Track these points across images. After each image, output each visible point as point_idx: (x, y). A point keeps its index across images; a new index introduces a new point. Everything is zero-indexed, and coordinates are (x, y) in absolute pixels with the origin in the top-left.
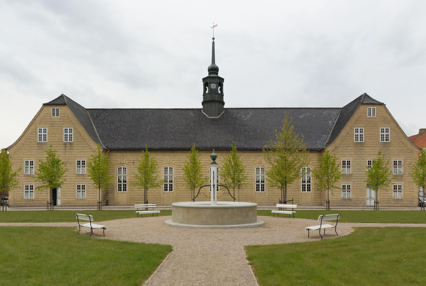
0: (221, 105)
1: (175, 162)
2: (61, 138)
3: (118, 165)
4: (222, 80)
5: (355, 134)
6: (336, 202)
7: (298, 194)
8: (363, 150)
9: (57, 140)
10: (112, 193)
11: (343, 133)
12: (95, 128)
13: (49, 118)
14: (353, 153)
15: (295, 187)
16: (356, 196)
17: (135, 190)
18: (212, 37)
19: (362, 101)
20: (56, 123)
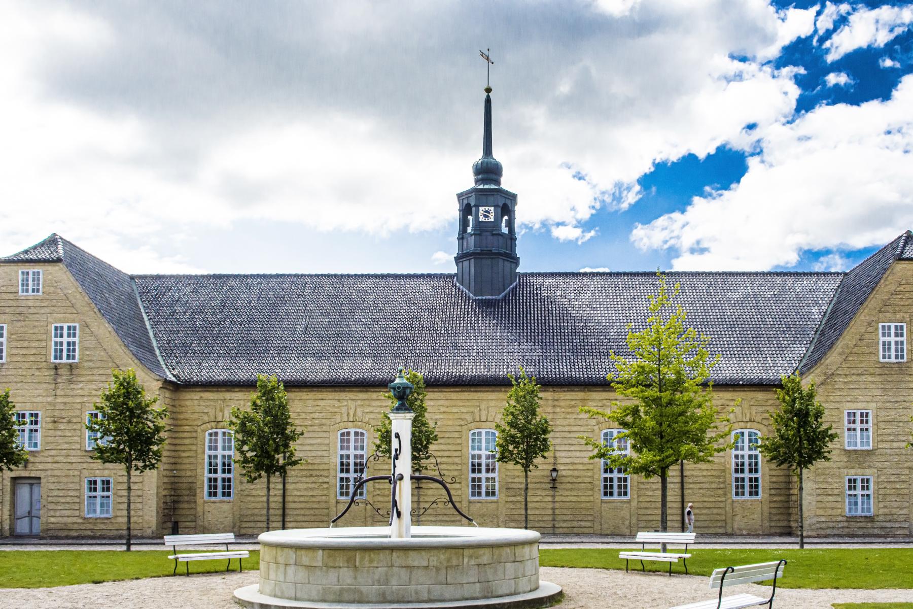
0: (507, 264)
1: (372, 416)
2: (44, 352)
3: (209, 425)
4: (513, 197)
5: (882, 339)
6: (831, 525)
7: (722, 505)
8: (903, 385)
9: (32, 358)
10: (188, 502)
11: (847, 339)
12: (148, 327)
13: (12, 296)
14: (879, 392)
15: (715, 486)
16: (885, 507)
17: (254, 492)
18: (486, 86)
19: (899, 251)
20: (32, 310)
